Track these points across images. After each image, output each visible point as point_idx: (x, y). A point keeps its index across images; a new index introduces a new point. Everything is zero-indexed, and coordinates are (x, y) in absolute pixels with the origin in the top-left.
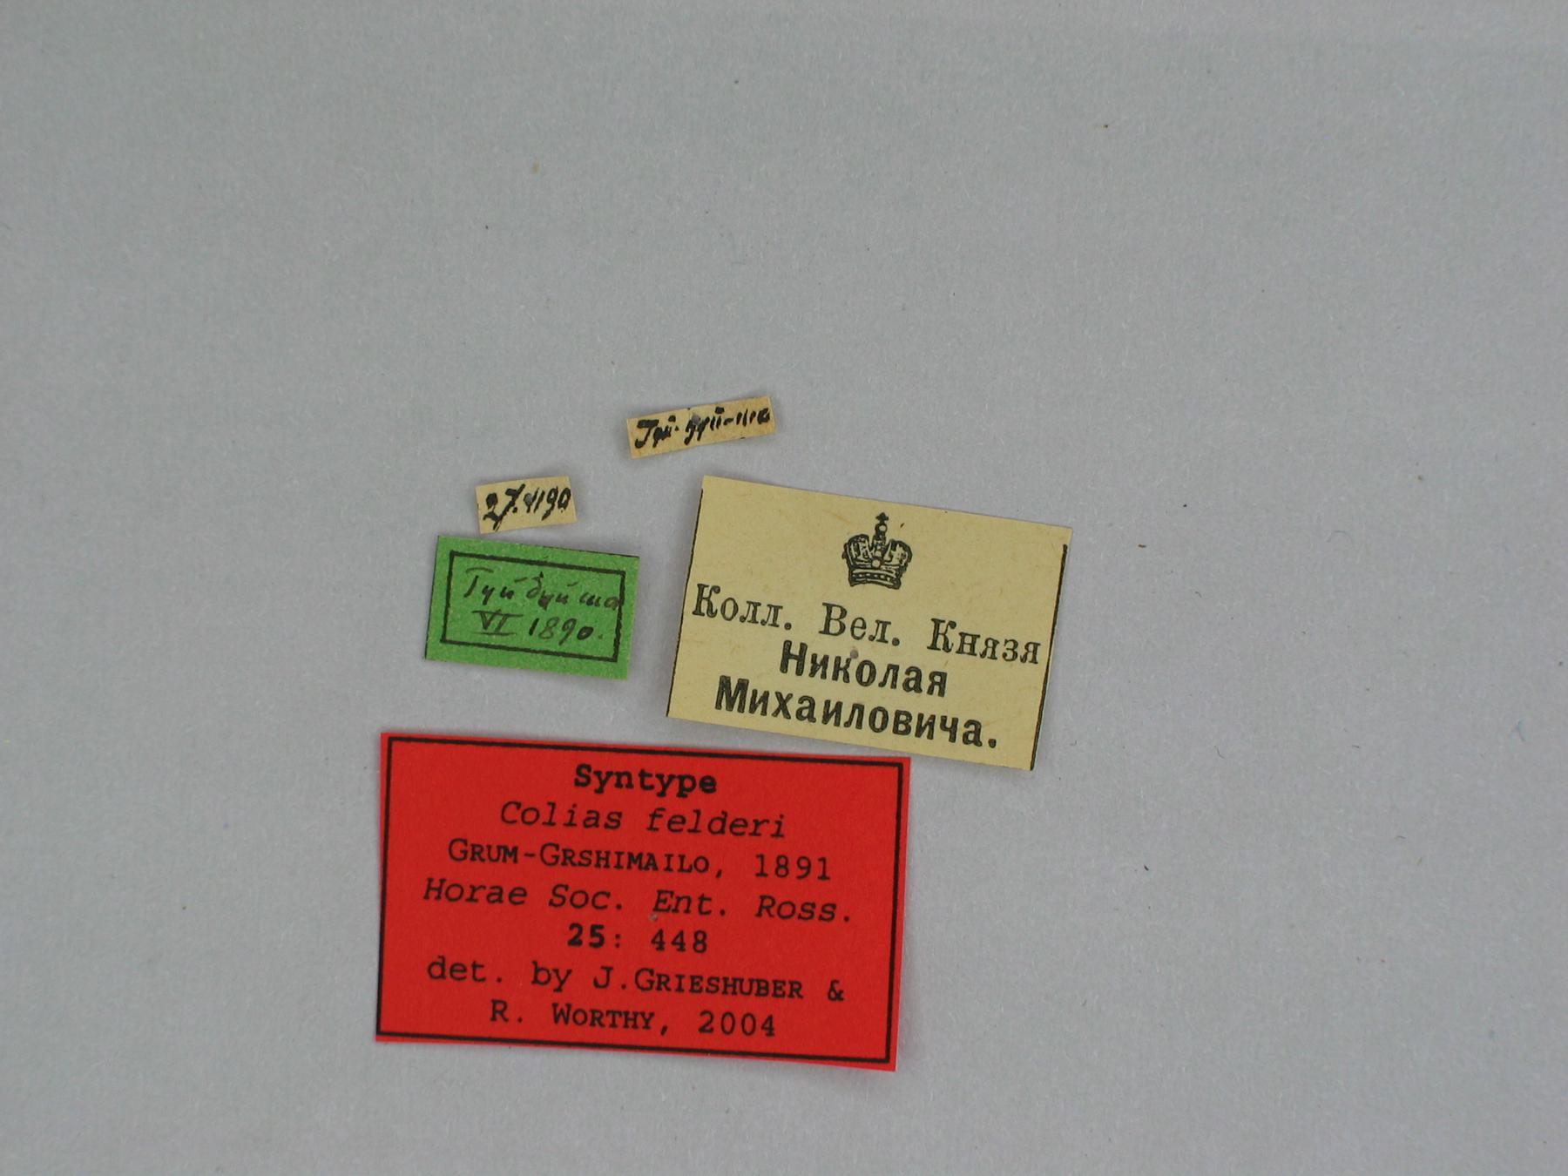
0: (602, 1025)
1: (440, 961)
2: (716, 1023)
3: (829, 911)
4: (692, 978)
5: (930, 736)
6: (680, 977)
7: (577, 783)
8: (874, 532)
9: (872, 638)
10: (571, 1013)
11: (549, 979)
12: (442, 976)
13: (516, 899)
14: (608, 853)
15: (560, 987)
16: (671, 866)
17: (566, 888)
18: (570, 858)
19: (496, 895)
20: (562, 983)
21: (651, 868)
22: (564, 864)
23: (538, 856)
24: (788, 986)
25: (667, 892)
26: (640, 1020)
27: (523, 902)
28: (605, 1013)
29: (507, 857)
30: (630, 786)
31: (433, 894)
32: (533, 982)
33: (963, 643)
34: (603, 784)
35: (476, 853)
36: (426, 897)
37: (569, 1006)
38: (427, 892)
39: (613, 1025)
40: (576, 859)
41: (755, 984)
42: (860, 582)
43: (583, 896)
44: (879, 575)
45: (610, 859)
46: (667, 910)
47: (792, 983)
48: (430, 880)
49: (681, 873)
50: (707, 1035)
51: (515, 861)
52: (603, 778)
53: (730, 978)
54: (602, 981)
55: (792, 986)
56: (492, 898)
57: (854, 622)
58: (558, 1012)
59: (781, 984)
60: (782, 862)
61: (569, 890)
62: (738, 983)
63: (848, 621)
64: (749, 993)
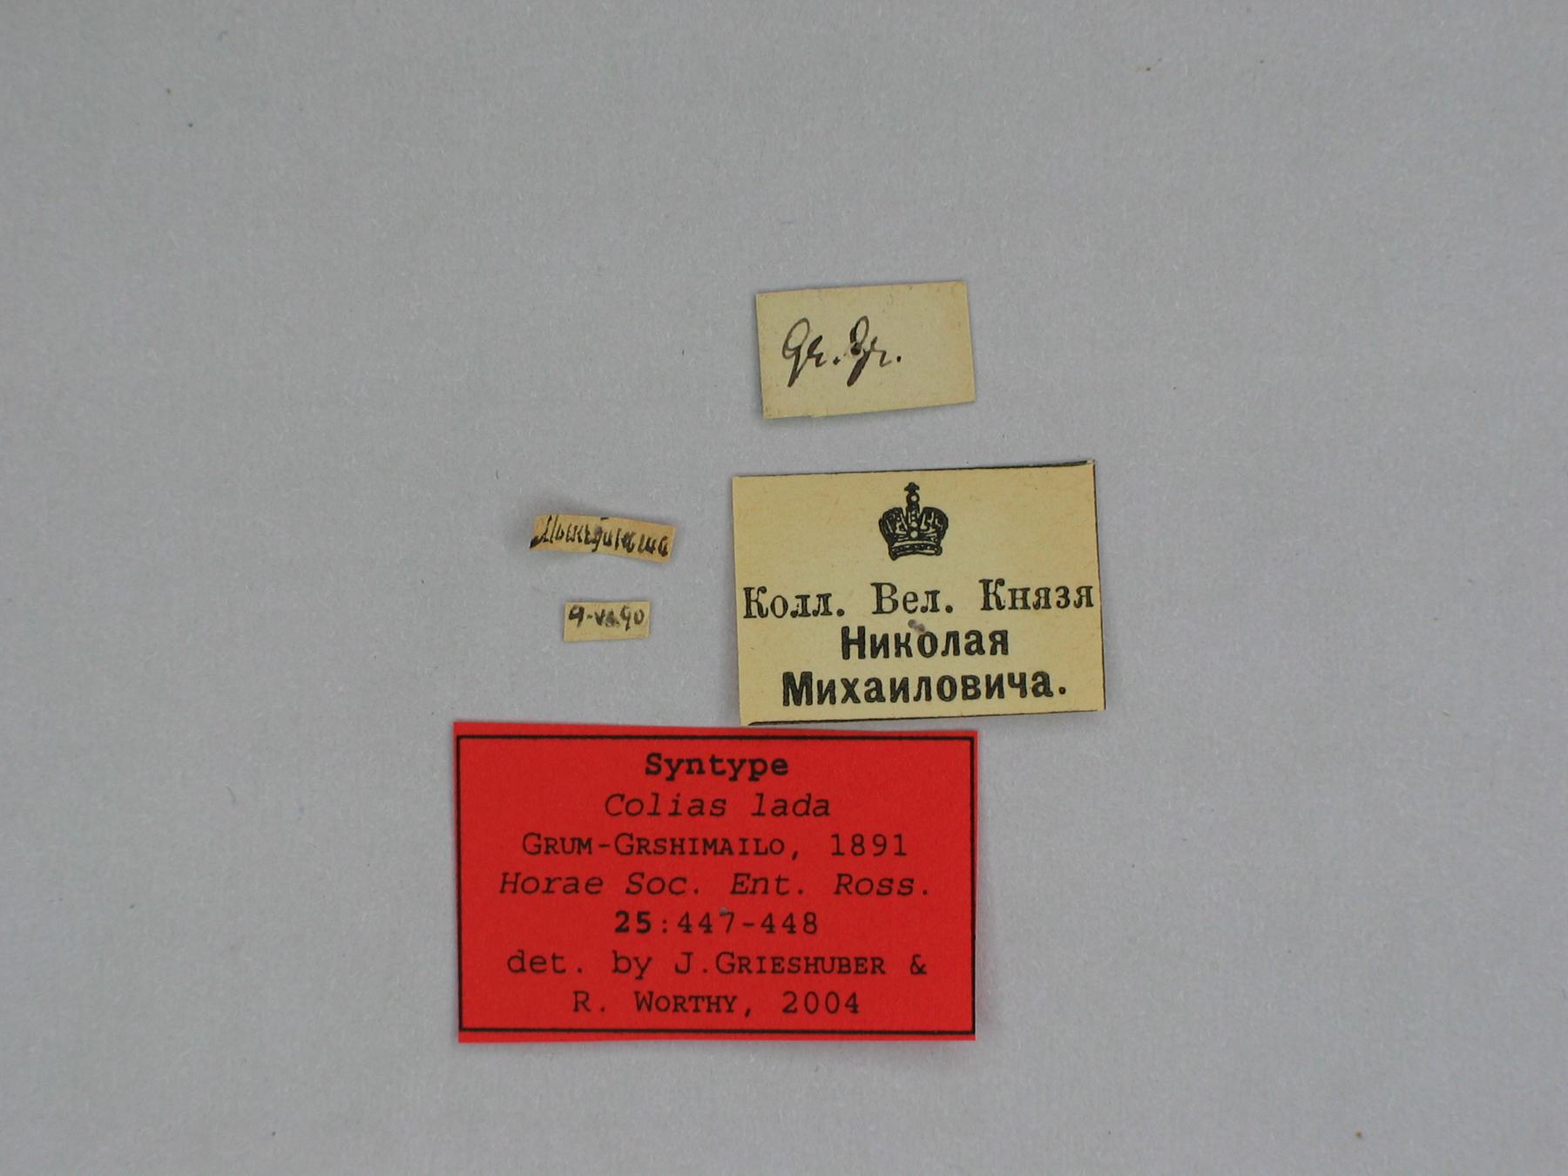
0: (685, 1011)
1: (520, 955)
2: (800, 1003)
3: (907, 887)
4: (774, 959)
6: (761, 959)
7: (648, 771)
9: (924, 609)
10: (654, 1002)
12: (523, 969)
13: (589, 888)
14: (682, 840)
17: (642, 875)
18: (645, 847)
19: (573, 886)
20: (643, 970)
21: (726, 852)
22: (639, 852)
23: (613, 846)
26: (724, 1006)
28: (687, 1000)
29: (582, 851)
30: (701, 771)
31: (509, 888)
34: (674, 771)
36: (502, 891)
37: (651, 994)
39: (697, 1010)
40: (651, 847)
44: (927, 545)
45: (684, 846)
46: (746, 892)
47: (873, 959)
48: (505, 875)
49: (756, 856)
51: (590, 853)
54: (682, 967)
56: (568, 889)
57: (905, 598)
58: (641, 998)
60: (858, 840)
61: (646, 875)
62: (820, 962)
63: (899, 597)
64: (832, 970)
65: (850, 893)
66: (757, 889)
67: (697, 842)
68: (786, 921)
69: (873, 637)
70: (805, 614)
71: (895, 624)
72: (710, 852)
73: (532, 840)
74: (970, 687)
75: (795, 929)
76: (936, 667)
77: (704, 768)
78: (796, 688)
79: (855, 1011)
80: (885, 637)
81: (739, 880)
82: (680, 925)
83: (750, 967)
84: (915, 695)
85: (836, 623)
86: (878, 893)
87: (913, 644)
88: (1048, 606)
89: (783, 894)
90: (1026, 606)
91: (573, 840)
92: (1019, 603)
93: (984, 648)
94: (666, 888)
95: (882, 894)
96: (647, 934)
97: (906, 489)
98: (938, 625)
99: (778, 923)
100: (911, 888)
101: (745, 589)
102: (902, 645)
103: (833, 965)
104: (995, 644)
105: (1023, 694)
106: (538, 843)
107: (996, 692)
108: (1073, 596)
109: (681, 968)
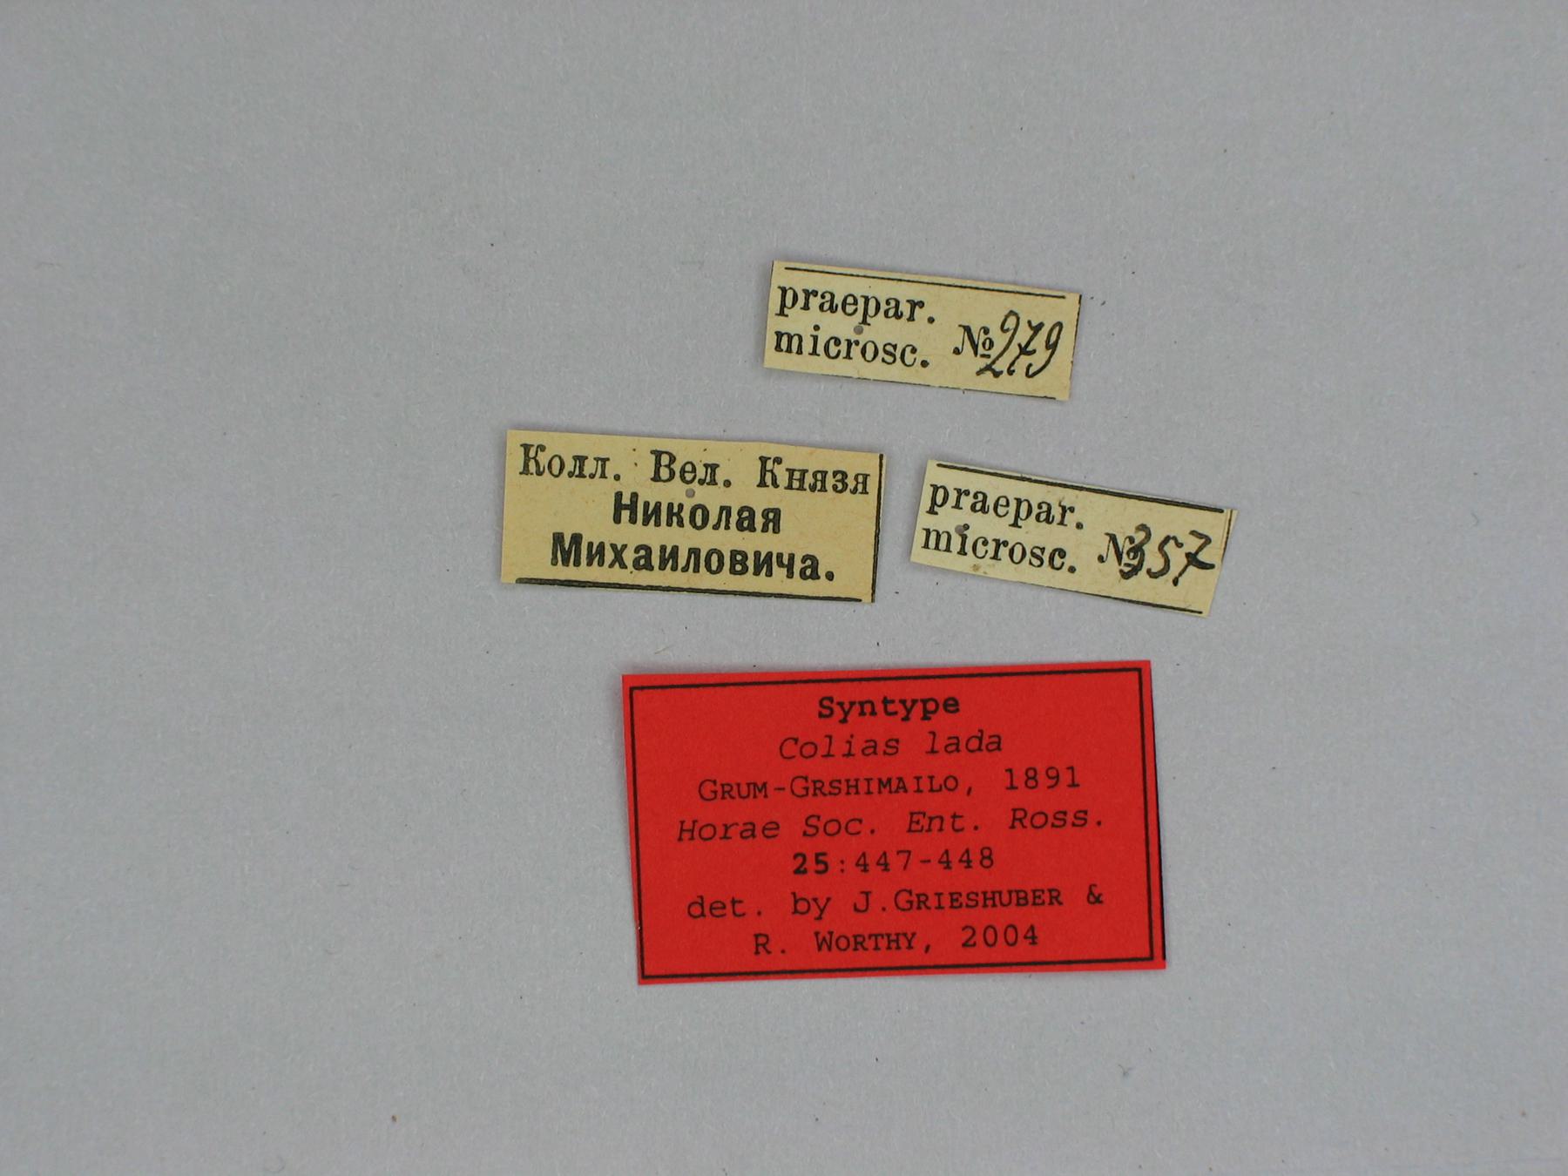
1: (700, 901)
2: (979, 938)
3: (1081, 818)
4: (951, 894)
5: (769, 574)
9: (702, 482)
10: (833, 942)
11: (809, 909)
12: (702, 914)
13: (766, 832)
14: (857, 780)
17: (819, 817)
19: (749, 831)
20: (822, 911)
21: (901, 791)
23: (788, 790)
24: (1047, 893)
25: (919, 813)
26: (903, 942)
27: (774, 836)
30: (873, 713)
31: (686, 835)
32: (793, 913)
33: (791, 478)
34: (846, 714)
35: (726, 791)
36: (680, 839)
37: (831, 933)
39: (876, 948)
40: (827, 789)
41: (1014, 895)
46: (921, 831)
47: (1050, 891)
48: (682, 822)
50: (972, 950)
51: (766, 796)
52: (846, 709)
54: (861, 906)
58: (820, 942)
59: (1040, 893)
61: (821, 818)
62: (997, 895)
65: (1024, 827)
66: (932, 827)
68: (963, 856)
73: (707, 789)
75: (971, 864)
77: (876, 709)
79: (1034, 943)
81: (915, 818)
82: (857, 865)
83: (928, 903)
84: (684, 565)
86: (1053, 825)
91: (748, 785)
94: (843, 826)
95: (1057, 827)
96: (823, 875)
98: (712, 498)
99: (954, 858)
100: (1085, 820)
106: (714, 788)
109: (858, 906)
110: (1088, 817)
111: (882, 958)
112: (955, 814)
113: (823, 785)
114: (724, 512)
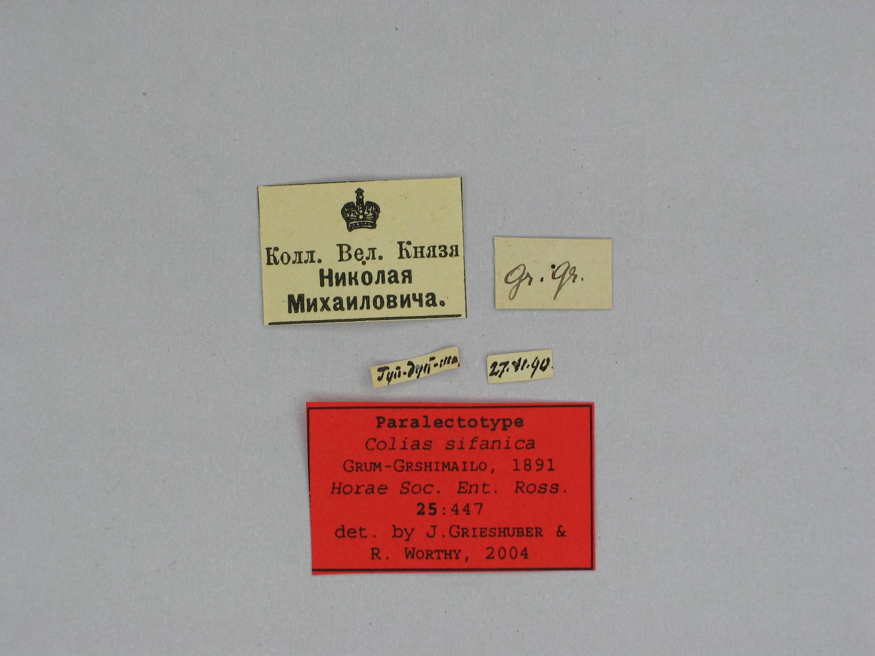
0: (432, 558)
1: (341, 528)
3: (555, 488)
4: (481, 529)
6: (474, 529)
8: (356, 200)
12: (343, 536)
13: (380, 491)
15: (409, 537)
16: (466, 468)
18: (410, 467)
19: (371, 490)
20: (409, 536)
21: (455, 470)
24: (534, 530)
27: (385, 493)
28: (434, 552)
29: (375, 467)
31: (336, 491)
36: (333, 493)
37: (414, 549)
38: (333, 490)
39: (439, 558)
40: (414, 467)
41: (516, 530)
42: (354, 229)
43: (418, 487)
44: (368, 223)
45: (432, 466)
46: (466, 492)
47: (536, 529)
48: (334, 484)
50: (491, 561)
51: (380, 470)
53: (502, 528)
54: (431, 534)
55: (536, 530)
56: (368, 491)
57: (357, 250)
60: (528, 462)
61: (411, 485)
62: (506, 530)
63: (352, 252)
64: (513, 535)
66: (472, 491)
67: (438, 465)
69: (337, 274)
70: (300, 262)
71: (353, 266)
72: (446, 469)
73: (348, 466)
74: (392, 301)
76: (373, 290)
78: (296, 303)
79: (526, 557)
80: (343, 274)
85: (317, 267)
87: (359, 278)
88: (434, 256)
89: (486, 493)
90: (422, 256)
91: (371, 463)
92: (419, 255)
93: (399, 280)
97: (356, 192)
98: (373, 267)
101: (267, 249)
102: (353, 279)
103: (514, 532)
104: (405, 277)
105: (421, 305)
106: (353, 465)
107: (406, 305)
108: (449, 251)
109: (430, 534)
110: (559, 488)
111: (443, 563)
112: (484, 484)
113: (412, 465)
114: (381, 274)
